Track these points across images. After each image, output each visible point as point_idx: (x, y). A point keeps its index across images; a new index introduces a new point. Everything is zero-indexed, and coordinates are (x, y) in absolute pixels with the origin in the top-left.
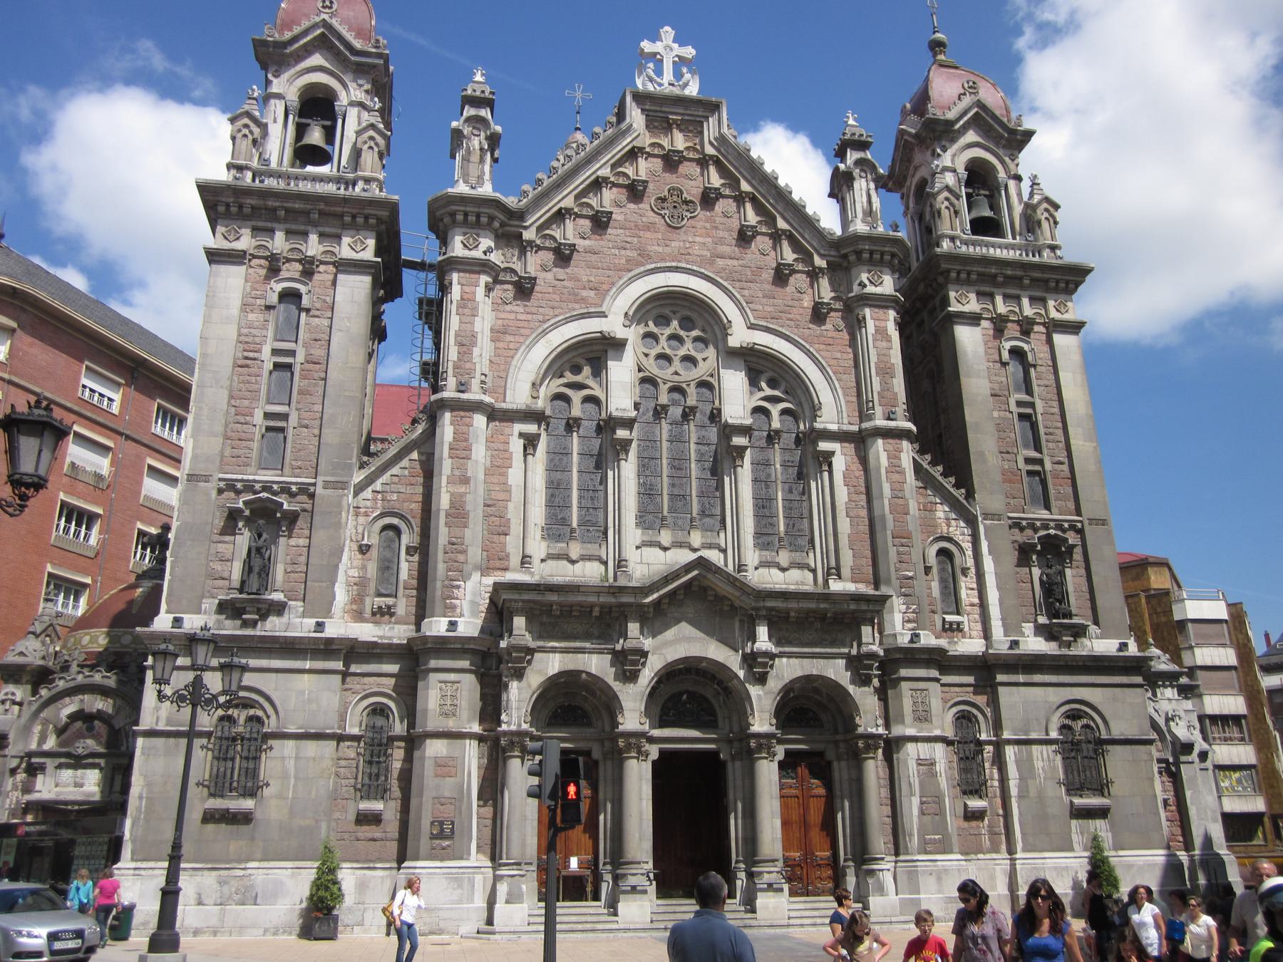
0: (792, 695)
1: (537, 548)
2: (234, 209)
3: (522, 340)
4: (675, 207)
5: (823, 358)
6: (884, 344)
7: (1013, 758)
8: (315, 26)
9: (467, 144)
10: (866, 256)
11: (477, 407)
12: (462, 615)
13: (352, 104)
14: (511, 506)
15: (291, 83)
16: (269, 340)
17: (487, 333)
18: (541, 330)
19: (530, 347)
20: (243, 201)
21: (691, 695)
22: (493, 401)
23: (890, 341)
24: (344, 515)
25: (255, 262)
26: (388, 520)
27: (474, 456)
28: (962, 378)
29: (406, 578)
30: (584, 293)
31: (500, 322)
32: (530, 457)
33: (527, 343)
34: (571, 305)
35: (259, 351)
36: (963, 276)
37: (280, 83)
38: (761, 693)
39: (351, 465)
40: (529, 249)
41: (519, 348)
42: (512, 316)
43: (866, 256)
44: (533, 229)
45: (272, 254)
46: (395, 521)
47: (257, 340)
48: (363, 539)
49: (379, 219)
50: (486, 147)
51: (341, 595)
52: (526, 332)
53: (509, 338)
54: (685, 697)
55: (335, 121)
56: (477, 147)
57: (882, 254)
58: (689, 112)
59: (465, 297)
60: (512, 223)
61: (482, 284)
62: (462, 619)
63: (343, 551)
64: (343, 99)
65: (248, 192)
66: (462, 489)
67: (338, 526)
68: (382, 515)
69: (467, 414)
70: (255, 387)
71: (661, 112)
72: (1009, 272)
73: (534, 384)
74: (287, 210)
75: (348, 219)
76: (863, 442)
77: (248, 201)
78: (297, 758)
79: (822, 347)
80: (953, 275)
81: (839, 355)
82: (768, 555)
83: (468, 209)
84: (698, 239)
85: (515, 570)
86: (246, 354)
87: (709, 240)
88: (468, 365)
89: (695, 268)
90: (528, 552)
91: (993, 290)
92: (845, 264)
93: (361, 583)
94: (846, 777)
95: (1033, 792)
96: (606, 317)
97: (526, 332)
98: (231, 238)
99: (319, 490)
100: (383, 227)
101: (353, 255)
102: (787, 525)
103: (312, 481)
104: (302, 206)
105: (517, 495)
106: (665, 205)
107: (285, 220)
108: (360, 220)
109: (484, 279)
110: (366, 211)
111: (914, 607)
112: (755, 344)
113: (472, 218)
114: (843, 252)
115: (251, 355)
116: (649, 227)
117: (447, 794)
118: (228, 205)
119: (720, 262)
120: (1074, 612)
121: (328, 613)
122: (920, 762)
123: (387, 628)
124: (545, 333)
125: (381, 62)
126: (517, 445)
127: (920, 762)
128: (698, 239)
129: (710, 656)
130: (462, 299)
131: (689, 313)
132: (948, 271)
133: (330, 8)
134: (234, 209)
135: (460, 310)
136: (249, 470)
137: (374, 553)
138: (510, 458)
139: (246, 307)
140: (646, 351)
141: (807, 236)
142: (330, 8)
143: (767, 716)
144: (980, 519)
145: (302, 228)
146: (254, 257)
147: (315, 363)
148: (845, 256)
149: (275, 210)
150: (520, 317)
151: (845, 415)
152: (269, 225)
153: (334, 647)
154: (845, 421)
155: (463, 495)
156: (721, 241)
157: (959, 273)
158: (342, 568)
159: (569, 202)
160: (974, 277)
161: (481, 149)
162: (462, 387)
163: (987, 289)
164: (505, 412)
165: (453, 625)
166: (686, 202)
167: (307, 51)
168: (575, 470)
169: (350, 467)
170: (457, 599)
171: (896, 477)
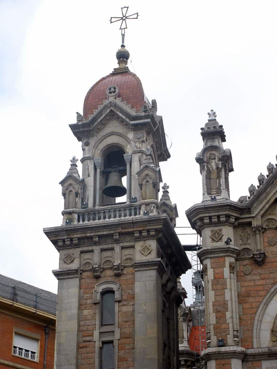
2: (68, 243)
3: (260, 299)
8: (106, 107)
9: (207, 167)
11: (234, 355)
13: (134, 153)
15: (96, 148)
16: (97, 327)
17: (235, 299)
18: (273, 290)
19: (267, 305)
20: (72, 236)
22: (243, 349)
25: (85, 274)
31: (244, 289)
33: (264, 301)
35: (92, 335)
37: (89, 150)
40: (257, 232)
41: (259, 306)
44: (259, 217)
45: (93, 268)
49: (156, 230)
50: (220, 166)
52: (262, 293)
53: (251, 300)
55: (125, 165)
56: (214, 167)
59: (217, 277)
61: (227, 265)
64: (129, 150)
65: (75, 230)
69: (227, 361)
70: (92, 360)
73: (272, 331)
75: (137, 235)
77: (75, 236)
83: (211, 214)
86: (84, 339)
88: (223, 326)
97: (262, 293)
98: (69, 261)
104: (108, 232)
108: (145, 234)
109: (229, 260)
110: (147, 228)
113: (215, 220)
115: (88, 339)
118: (64, 241)
125: (149, 120)
130: (215, 278)
133: (114, 92)
134: (68, 243)
135: (214, 286)
139: (81, 306)
142: (114, 92)
145: (110, 246)
146: (84, 271)
147: (127, 338)
150: (257, 283)
152: (90, 248)
161: (217, 168)
162: (222, 343)
164: (254, 355)
167: (103, 124)
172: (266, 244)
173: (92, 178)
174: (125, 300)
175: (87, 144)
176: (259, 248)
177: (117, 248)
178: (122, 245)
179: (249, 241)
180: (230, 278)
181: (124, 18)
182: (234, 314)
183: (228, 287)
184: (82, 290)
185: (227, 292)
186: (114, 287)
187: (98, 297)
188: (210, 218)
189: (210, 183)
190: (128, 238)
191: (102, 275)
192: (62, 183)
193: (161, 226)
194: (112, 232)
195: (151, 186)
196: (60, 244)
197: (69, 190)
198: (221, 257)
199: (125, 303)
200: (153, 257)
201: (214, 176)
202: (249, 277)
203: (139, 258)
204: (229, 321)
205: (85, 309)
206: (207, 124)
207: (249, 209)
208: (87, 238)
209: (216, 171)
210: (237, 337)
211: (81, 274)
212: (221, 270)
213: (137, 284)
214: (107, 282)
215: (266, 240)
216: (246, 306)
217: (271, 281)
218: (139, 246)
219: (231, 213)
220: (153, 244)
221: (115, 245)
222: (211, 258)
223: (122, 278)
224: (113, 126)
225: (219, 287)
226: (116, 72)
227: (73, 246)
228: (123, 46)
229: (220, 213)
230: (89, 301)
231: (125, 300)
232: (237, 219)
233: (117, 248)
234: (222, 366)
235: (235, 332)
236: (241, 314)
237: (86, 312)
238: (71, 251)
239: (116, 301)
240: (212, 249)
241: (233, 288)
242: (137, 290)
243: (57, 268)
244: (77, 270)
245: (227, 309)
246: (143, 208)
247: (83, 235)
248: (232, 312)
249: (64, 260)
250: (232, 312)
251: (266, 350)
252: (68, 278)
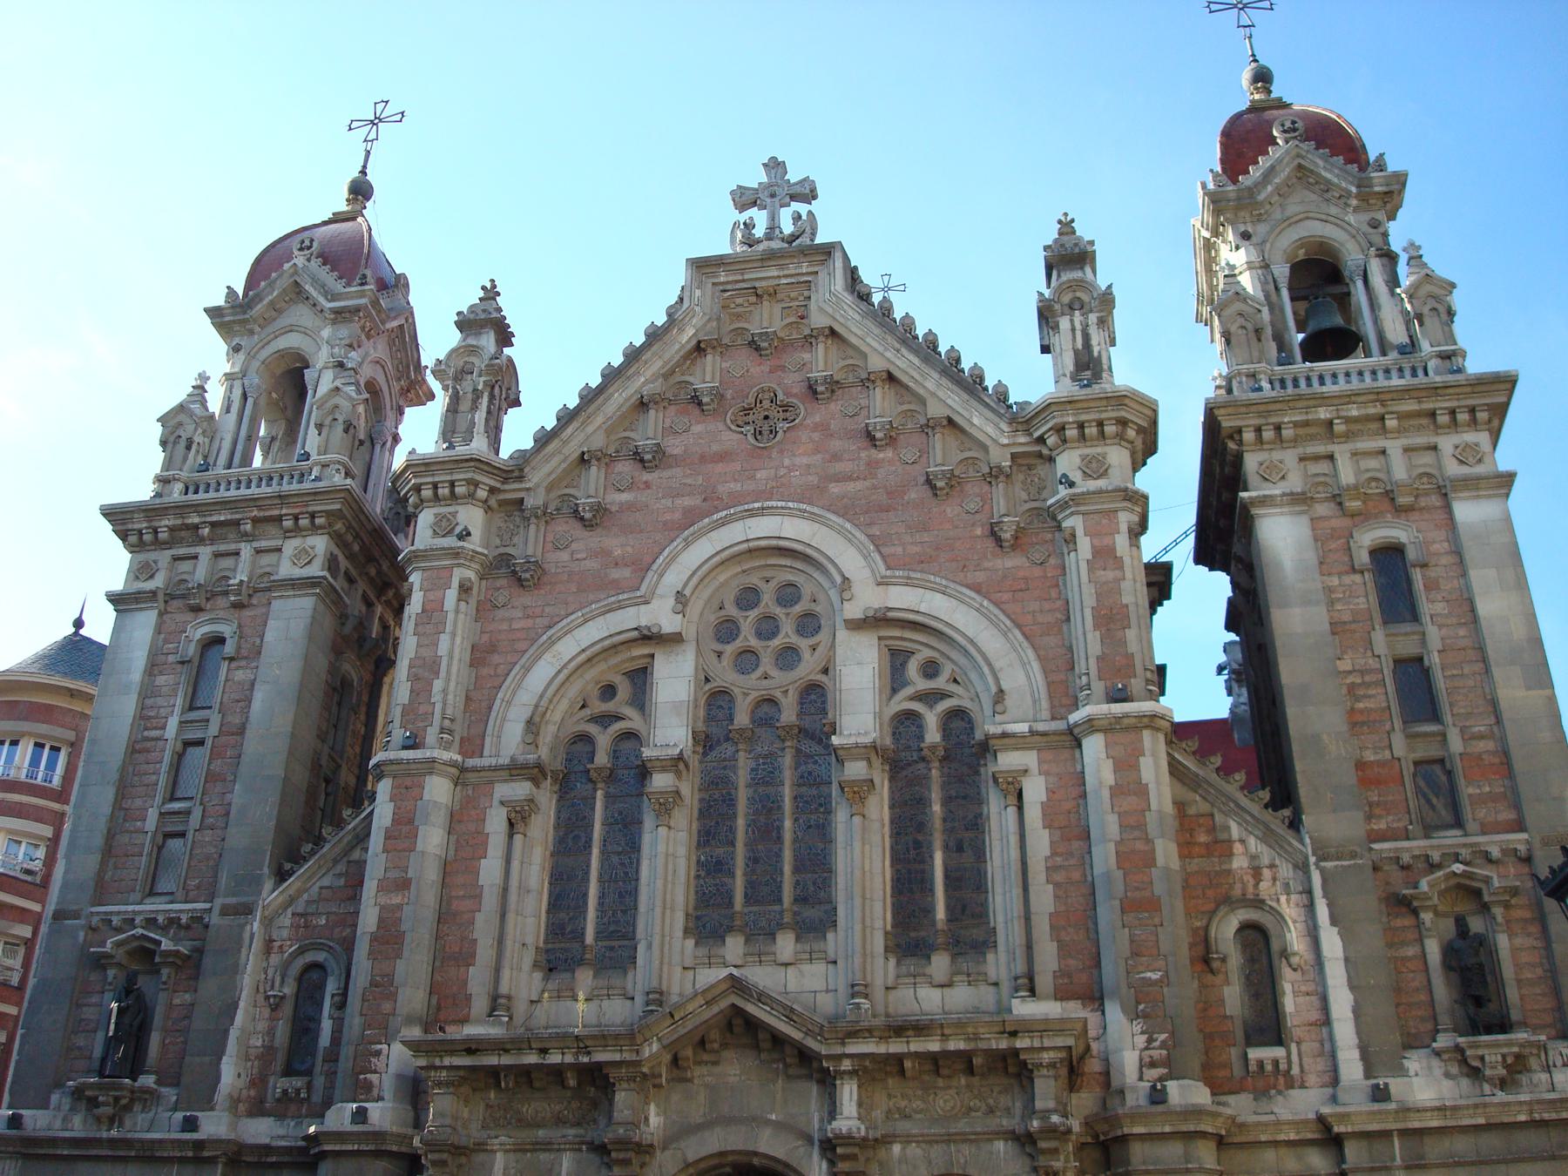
1: (523, 981)
2: (147, 538)
4: (766, 417)
5: (1008, 616)
6: (1110, 575)
9: (454, 388)
10: (1071, 433)
12: (380, 1098)
14: (480, 918)
16: (177, 710)
23: (1121, 568)
24: (244, 951)
26: (310, 957)
27: (420, 846)
28: (1272, 610)
29: (328, 1044)
30: (615, 574)
31: (485, 638)
32: (518, 838)
34: (591, 597)
35: (164, 728)
36: (1268, 434)
39: (261, 875)
40: (533, 520)
42: (505, 626)
43: (1071, 433)
44: (542, 491)
46: (320, 957)
47: (163, 712)
48: (272, 988)
51: (230, 1074)
52: (521, 646)
53: (496, 659)
57: (1100, 424)
58: (786, 272)
59: (428, 608)
60: (506, 487)
61: (455, 583)
62: (380, 1104)
63: (237, 1008)
66: (396, 899)
67: (235, 970)
68: (301, 951)
71: (743, 281)
72: (1355, 413)
74: (213, 525)
75: (288, 524)
76: (1080, 746)
77: (163, 523)
79: (1006, 596)
80: (1249, 436)
81: (1035, 606)
82: (911, 964)
83: (437, 479)
84: (797, 461)
85: (478, 1022)
87: (819, 456)
89: (790, 505)
90: (504, 989)
91: (1331, 448)
92: (1045, 452)
93: (269, 1051)
96: (647, 603)
98: (144, 576)
99: (215, 919)
100: (339, 526)
101: (297, 572)
102: (948, 908)
103: (208, 906)
105: (490, 901)
106: (750, 418)
107: (212, 540)
108: (304, 522)
110: (310, 509)
111: (1163, 1036)
112: (890, 609)
114: (1036, 435)
116: (723, 457)
118: (140, 533)
119: (835, 489)
120: (1515, 1015)
121: (209, 1105)
123: (292, 1124)
124: (552, 642)
126: (496, 822)
128: (797, 461)
129: (763, 1148)
131: (790, 577)
132: (1239, 431)
134: (147, 538)
136: (137, 896)
137: (287, 1009)
138: (485, 843)
139: (154, 666)
140: (719, 647)
141: (976, 421)
144: (1312, 859)
145: (233, 547)
148: (1041, 440)
149: (196, 527)
151: (1045, 704)
152: (192, 550)
153: (206, 1154)
154: (1046, 714)
155: (400, 907)
156: (836, 457)
157: (1258, 430)
158: (234, 1034)
159: (598, 442)
160: (1287, 433)
161: (475, 390)
163: (1320, 448)
165: (361, 1116)
166: (786, 407)
168: (595, 851)
169: (257, 882)
170: (375, 1072)
171: (1130, 802)
172: (549, 546)
173: (233, 416)
174: (246, 658)
175: (236, 349)
176: (530, 552)
177: (246, 550)
178: (255, 544)
179: (515, 540)
180: (457, 611)
181: (375, 122)
182: (452, 684)
183: (448, 628)
184: (162, 636)
185: (444, 643)
186: (226, 630)
187: (192, 650)
188: (435, 486)
189: (454, 421)
190: (272, 529)
191: (208, 606)
192: (163, 420)
193: (338, 506)
194: (237, 516)
195: (340, 428)
196: (133, 539)
197: (176, 434)
198: (445, 567)
199: (243, 663)
200: (316, 570)
201: (465, 405)
202: (500, 613)
203: (287, 569)
204: (437, 697)
205: (161, 673)
206: (472, 308)
207: (521, 470)
208: (187, 527)
209: (470, 396)
210: (450, 732)
211: (166, 602)
212: (439, 594)
213: (271, 623)
214: (212, 621)
215: (550, 537)
216: (485, 671)
217: (546, 621)
218: (290, 546)
219: (479, 477)
220: (320, 544)
221: (243, 545)
222: (424, 570)
223: (247, 613)
224: (300, 315)
225: (429, 629)
226: (337, 218)
227: (158, 544)
228: (363, 172)
229: (456, 477)
230: (171, 658)
231: (246, 658)
232: (492, 490)
233: (246, 550)
234: (403, 791)
235: (447, 723)
236: (472, 687)
237: (161, 680)
238: (152, 556)
239: (224, 659)
240: (426, 551)
241: (459, 632)
242: (269, 637)
243: (118, 585)
244: (154, 593)
245: (437, 674)
246: (315, 473)
247: (179, 522)
248: (448, 680)
249: (140, 571)
250: (448, 680)
251: (507, 761)
252: (137, 609)
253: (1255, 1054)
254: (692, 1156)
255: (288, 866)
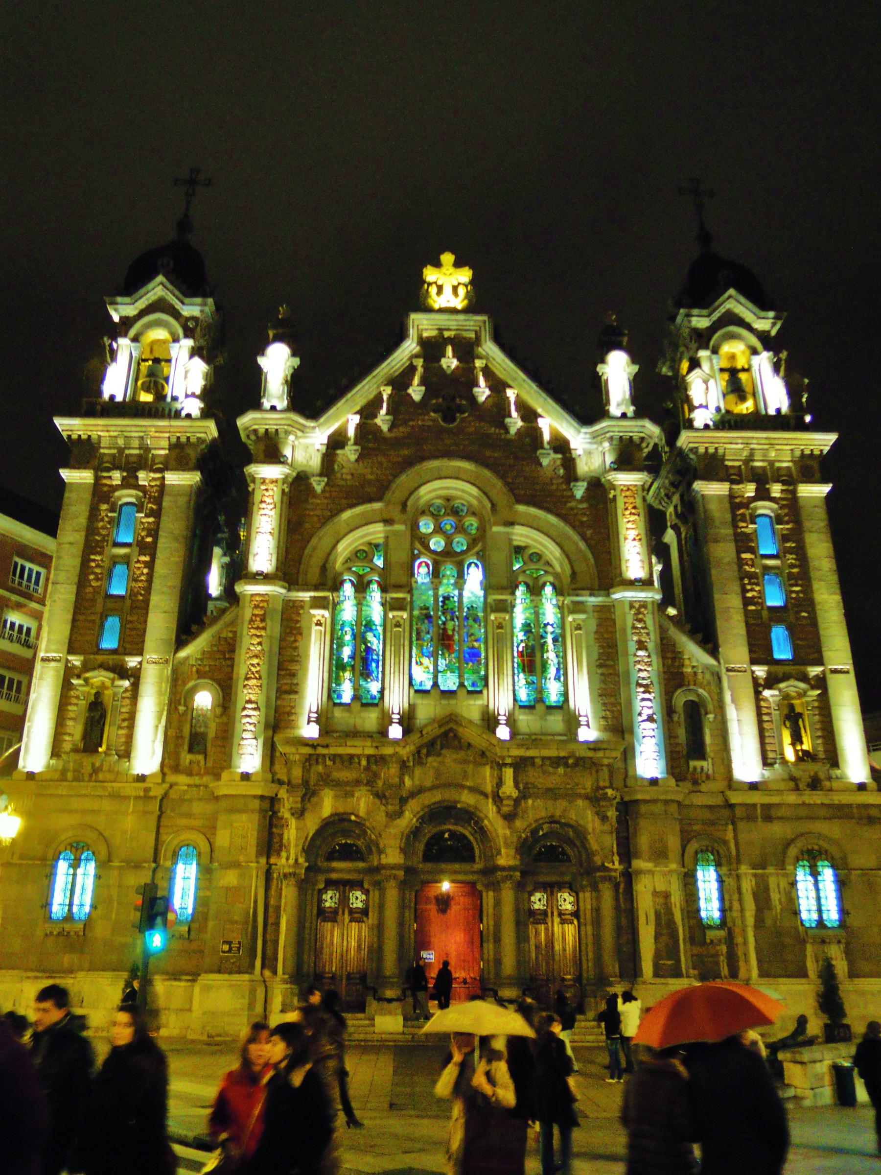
0: (541, 833)
7: (750, 892)
21: (453, 834)
38: (508, 832)
54: (446, 835)
78: (120, 886)
94: (589, 907)
95: (769, 922)
117: (236, 918)
122: (655, 893)
127: (655, 893)
143: (512, 852)
253: (693, 763)
254: (427, 802)
255: (184, 637)
